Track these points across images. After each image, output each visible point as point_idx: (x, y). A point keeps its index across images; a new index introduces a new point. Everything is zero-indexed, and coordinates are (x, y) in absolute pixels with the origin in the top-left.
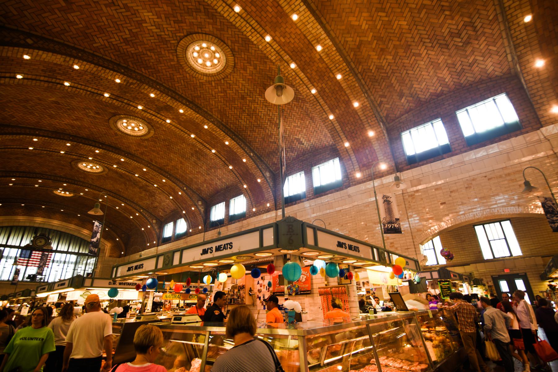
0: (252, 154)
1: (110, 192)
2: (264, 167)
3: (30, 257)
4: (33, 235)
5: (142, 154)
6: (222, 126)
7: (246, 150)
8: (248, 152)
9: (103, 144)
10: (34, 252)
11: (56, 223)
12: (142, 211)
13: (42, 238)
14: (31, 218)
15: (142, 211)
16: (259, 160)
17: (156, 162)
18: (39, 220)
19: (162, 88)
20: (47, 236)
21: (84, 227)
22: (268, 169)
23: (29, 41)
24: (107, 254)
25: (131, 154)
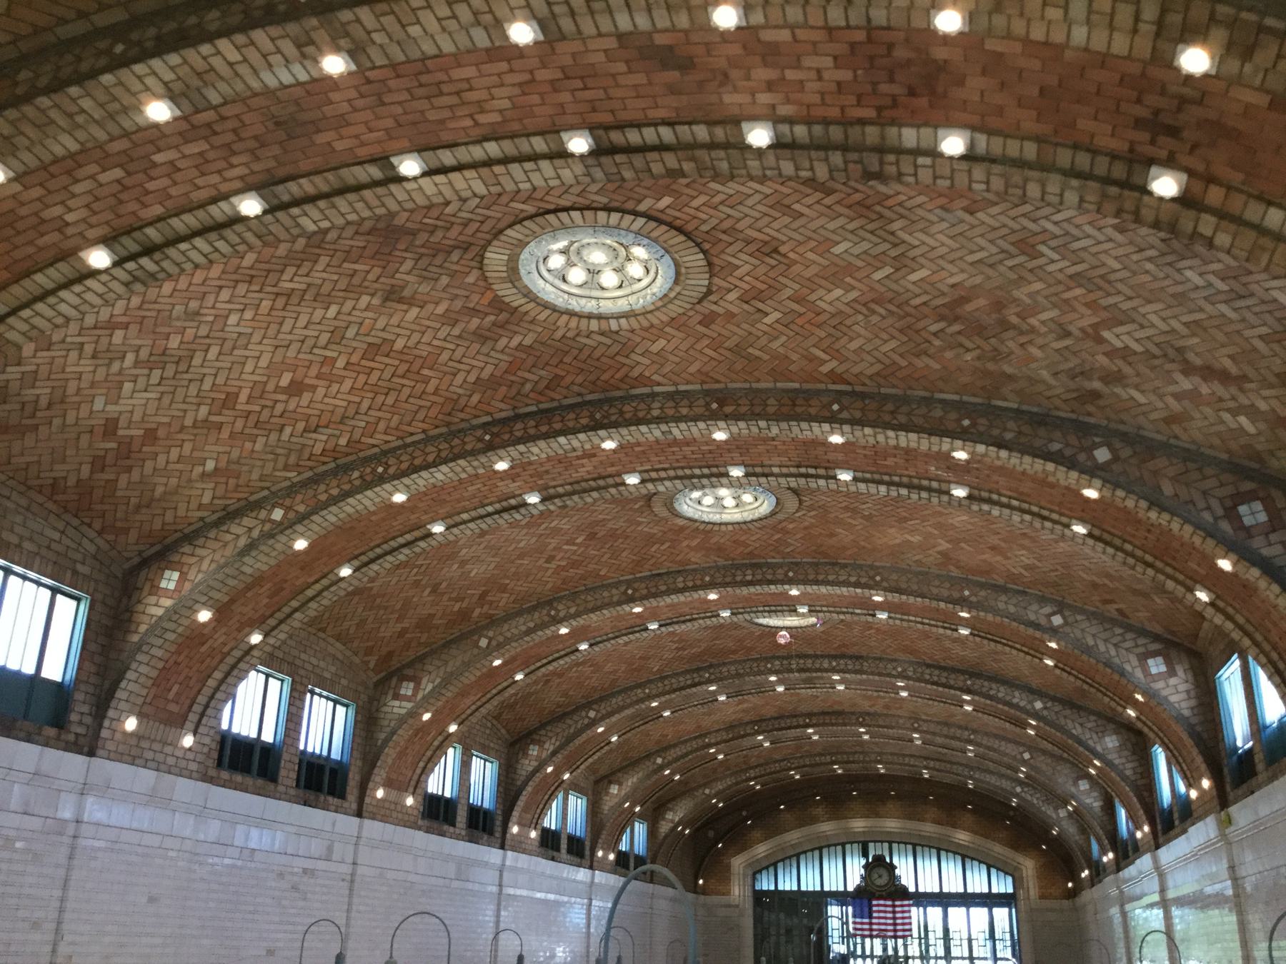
0: (1039, 705)
1: (926, 758)
2: (1089, 725)
3: (871, 917)
4: (863, 862)
5: (887, 707)
6: (928, 671)
7: (1015, 701)
8: (1022, 704)
9: (810, 715)
10: (875, 902)
11: (892, 824)
12: (1018, 789)
13: (879, 866)
14: (843, 823)
15: (1018, 789)
16: (1068, 712)
17: (926, 714)
18: (859, 825)
19: (777, 663)
20: (888, 860)
21: (954, 826)
22: (1112, 726)
23: (592, 714)
24: (1034, 892)
25: (868, 714)
